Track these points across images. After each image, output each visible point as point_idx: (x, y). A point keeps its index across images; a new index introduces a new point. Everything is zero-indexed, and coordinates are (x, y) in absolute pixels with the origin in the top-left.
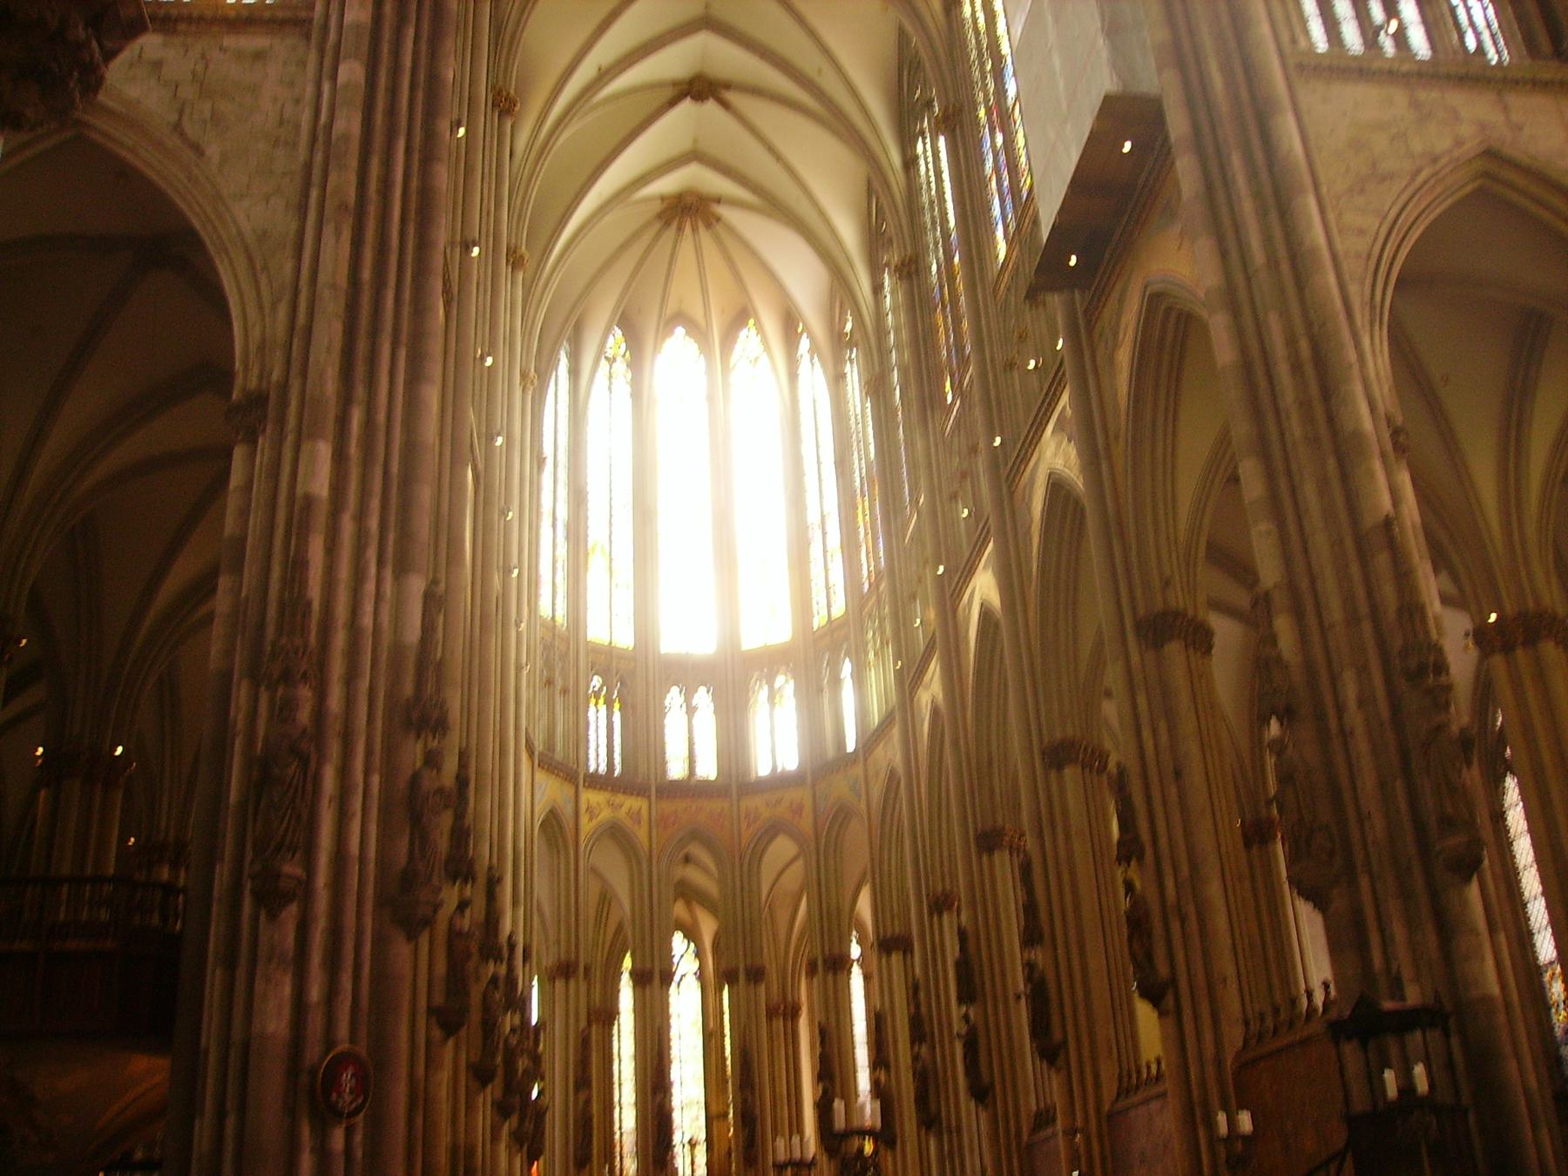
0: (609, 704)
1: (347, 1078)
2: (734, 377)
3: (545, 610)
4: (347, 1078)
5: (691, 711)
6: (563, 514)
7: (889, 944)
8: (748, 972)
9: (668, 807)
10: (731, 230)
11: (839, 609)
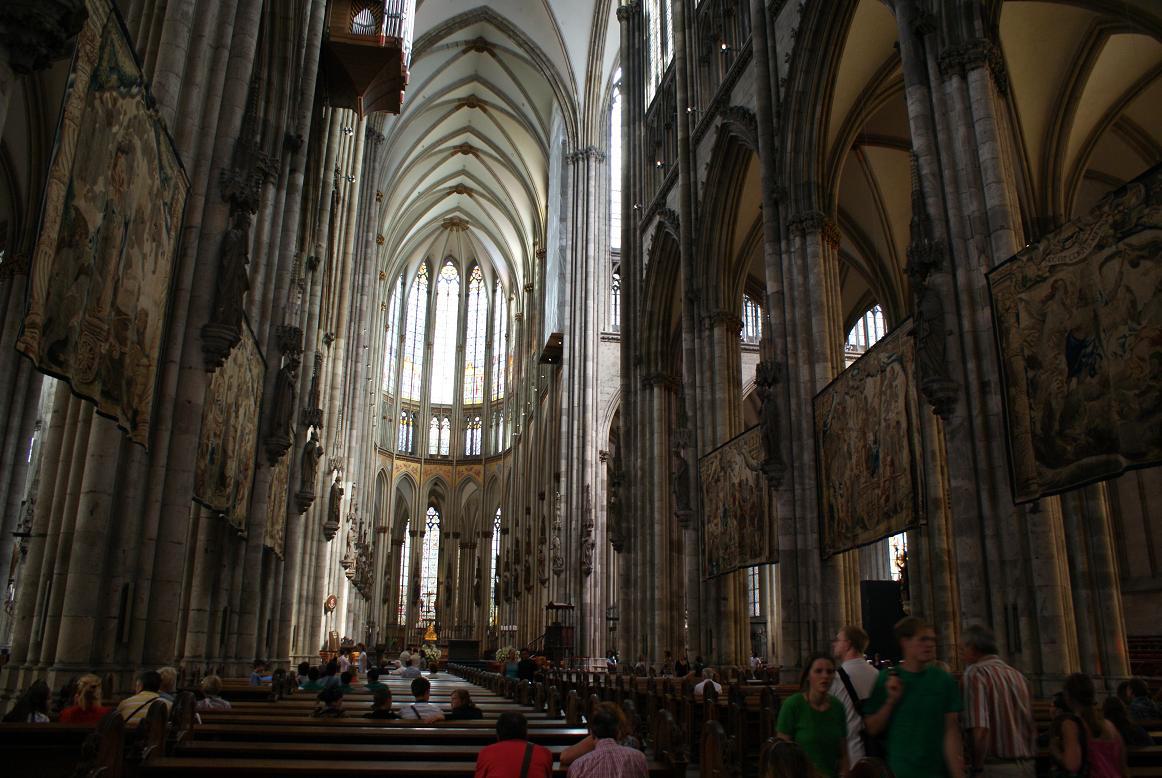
0: (408, 425)
1: (332, 601)
2: (471, 286)
3: (385, 388)
4: (332, 601)
5: (440, 428)
6: (395, 346)
7: (504, 531)
8: (453, 533)
9: (430, 467)
10: (472, 232)
11: (501, 396)
